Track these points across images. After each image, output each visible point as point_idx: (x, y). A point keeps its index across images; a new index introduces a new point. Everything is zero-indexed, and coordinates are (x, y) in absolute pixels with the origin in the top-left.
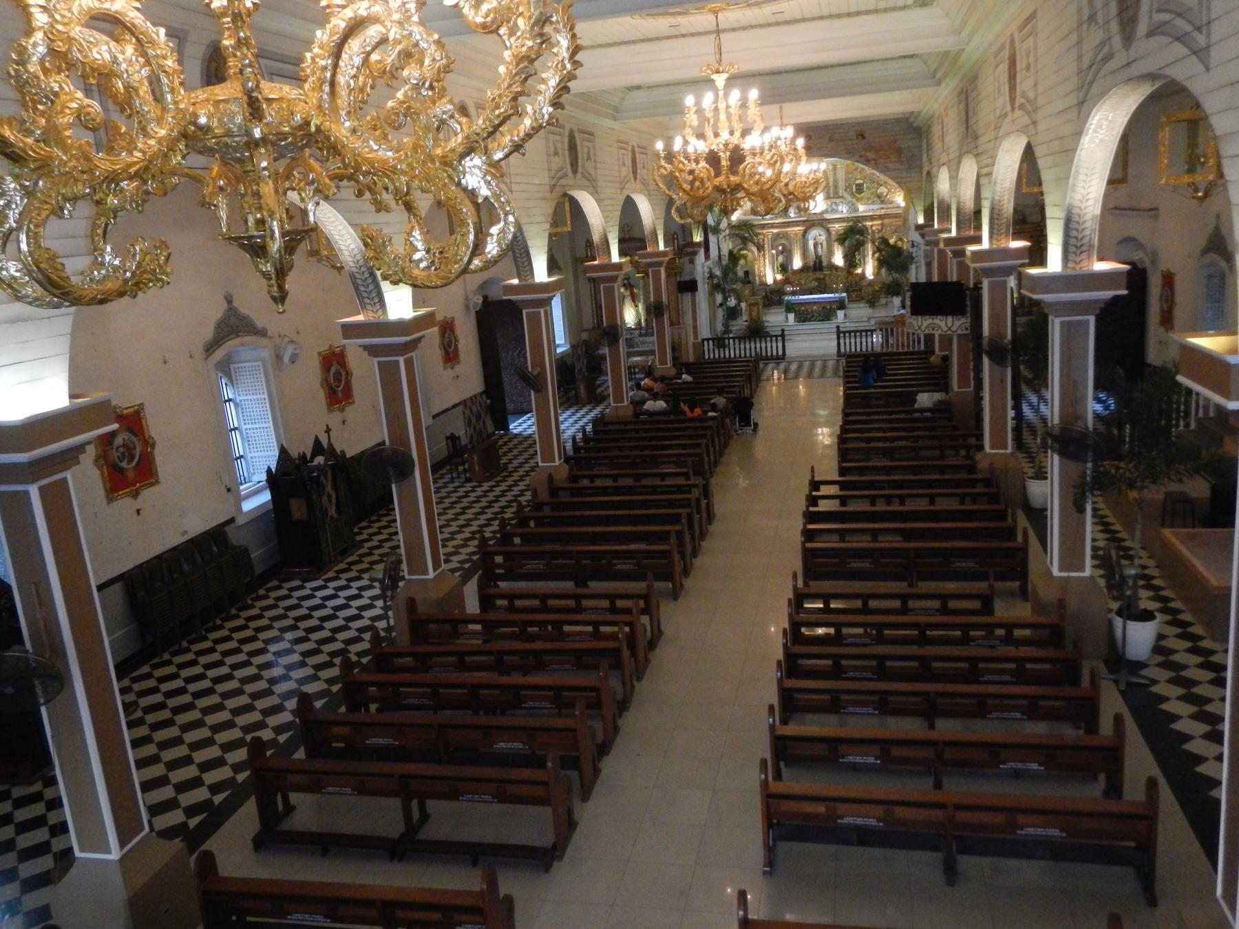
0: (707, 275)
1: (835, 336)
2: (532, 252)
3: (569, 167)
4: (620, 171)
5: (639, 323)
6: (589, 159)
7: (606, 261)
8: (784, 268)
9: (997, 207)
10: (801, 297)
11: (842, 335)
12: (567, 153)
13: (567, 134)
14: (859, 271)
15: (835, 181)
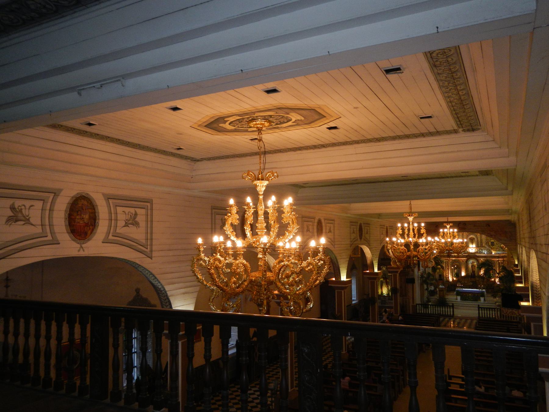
0: (420, 276)
1: (477, 309)
2: (341, 269)
3: (358, 237)
4: (380, 237)
5: (388, 294)
6: (367, 233)
7: (372, 271)
8: (458, 275)
9: (526, 270)
10: (464, 289)
11: (480, 309)
12: (358, 232)
13: (359, 225)
14: (493, 280)
15: (481, 240)
